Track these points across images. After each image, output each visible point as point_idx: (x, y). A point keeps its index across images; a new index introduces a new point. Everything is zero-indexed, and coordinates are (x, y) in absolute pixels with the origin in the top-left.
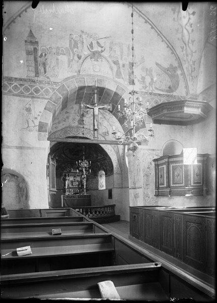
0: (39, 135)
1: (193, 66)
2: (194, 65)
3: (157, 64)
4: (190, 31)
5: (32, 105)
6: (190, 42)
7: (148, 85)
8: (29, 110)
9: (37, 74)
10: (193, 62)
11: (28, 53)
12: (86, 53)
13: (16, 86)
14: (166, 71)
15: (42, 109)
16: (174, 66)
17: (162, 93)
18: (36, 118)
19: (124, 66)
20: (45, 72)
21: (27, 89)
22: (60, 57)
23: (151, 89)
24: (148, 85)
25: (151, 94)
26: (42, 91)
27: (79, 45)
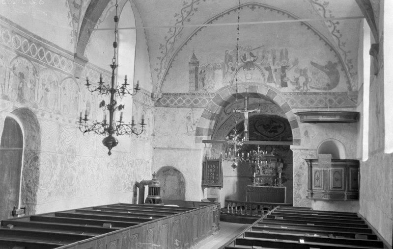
0: (196, 138)
1: (350, 65)
2: (351, 63)
3: (313, 64)
4: (339, 36)
6: (341, 44)
7: (301, 85)
9: (197, 87)
10: (348, 61)
11: (191, 72)
14: (322, 68)
15: (199, 116)
16: (333, 62)
17: (317, 91)
18: (194, 124)
19: (276, 70)
20: (204, 85)
21: (188, 101)
23: (305, 88)
24: (301, 85)
25: (305, 94)
27: (234, 58)
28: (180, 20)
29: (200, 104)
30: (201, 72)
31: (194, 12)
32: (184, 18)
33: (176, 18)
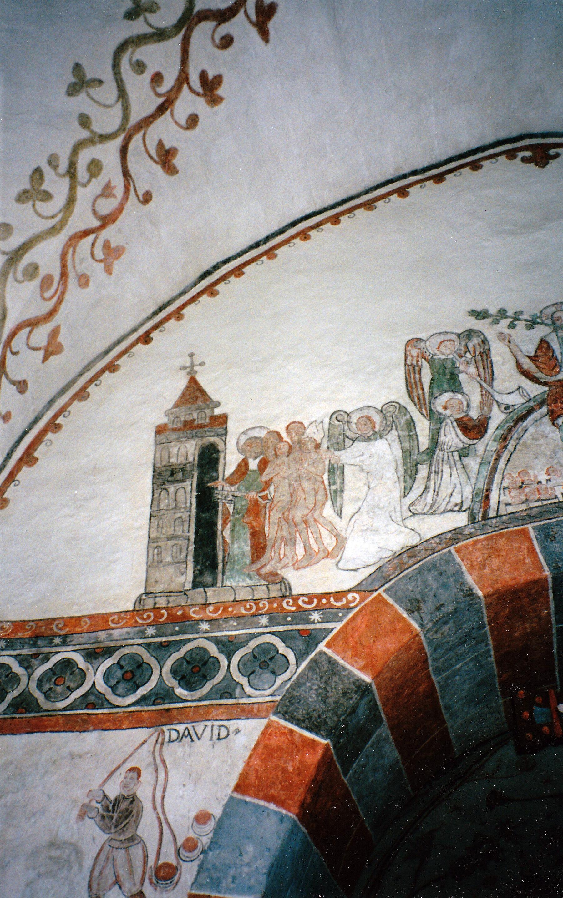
5: (147, 776)
8: (127, 814)
9: (207, 558)
11: (165, 476)
12: (516, 400)
13: (68, 663)
20: (259, 548)
22: (349, 456)
26: (230, 667)
28: (108, 120)
29: (227, 690)
30: (243, 468)
31: (200, 106)
32: (134, 119)
33: (81, 103)
